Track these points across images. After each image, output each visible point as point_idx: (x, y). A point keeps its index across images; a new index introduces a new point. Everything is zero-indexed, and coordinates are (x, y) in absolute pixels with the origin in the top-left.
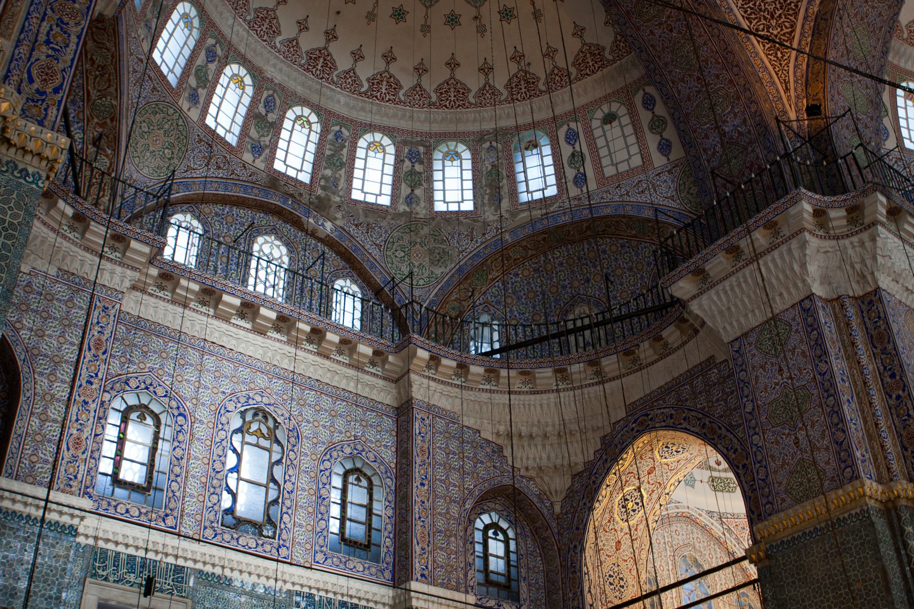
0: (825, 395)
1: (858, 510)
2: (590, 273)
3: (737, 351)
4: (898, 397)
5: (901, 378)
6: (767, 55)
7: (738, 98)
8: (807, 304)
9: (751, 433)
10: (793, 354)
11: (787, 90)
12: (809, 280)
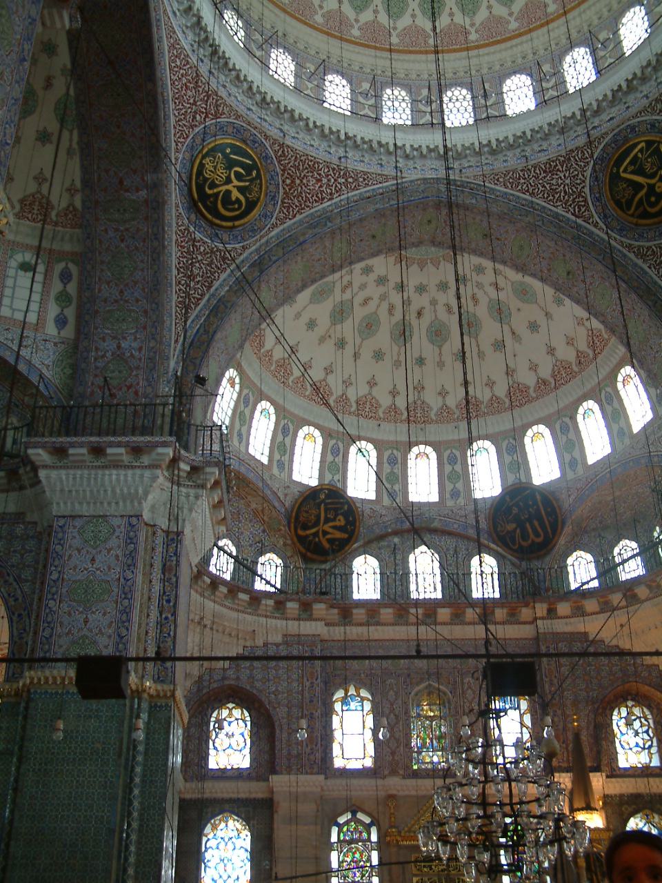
0: (123, 596)
3: (60, 527)
4: (166, 618)
6: (177, 306)
8: (134, 521)
9: (49, 597)
10: (108, 553)
11: (176, 341)
12: (144, 504)
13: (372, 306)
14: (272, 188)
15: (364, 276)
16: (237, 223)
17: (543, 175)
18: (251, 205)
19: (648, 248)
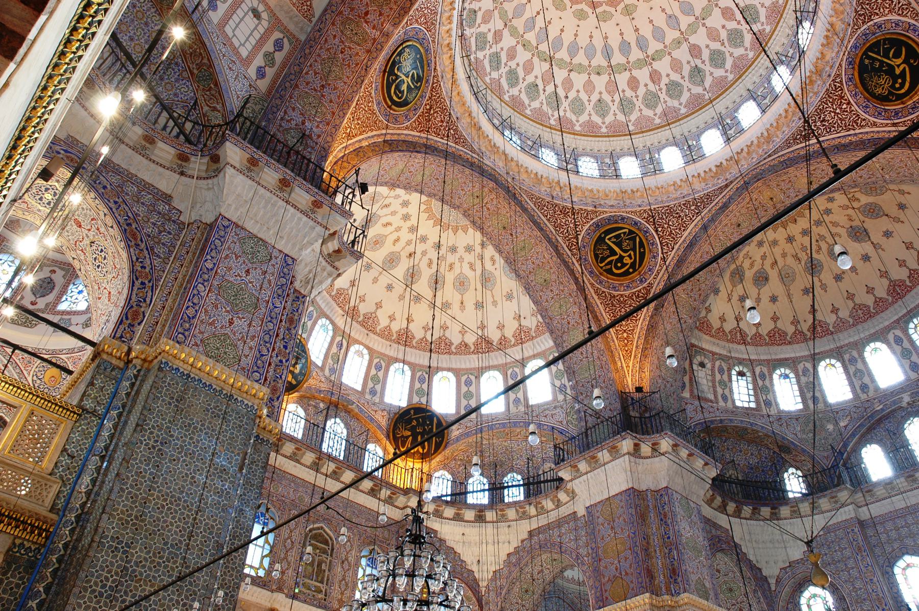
1: (250, 404)
2: (138, 40)
4: (281, 361)
5: (289, 353)
7: (328, 124)
13: (390, 229)
14: (418, 103)
15: (405, 208)
16: (393, 107)
17: (559, 213)
18: (405, 103)
19: (603, 292)
